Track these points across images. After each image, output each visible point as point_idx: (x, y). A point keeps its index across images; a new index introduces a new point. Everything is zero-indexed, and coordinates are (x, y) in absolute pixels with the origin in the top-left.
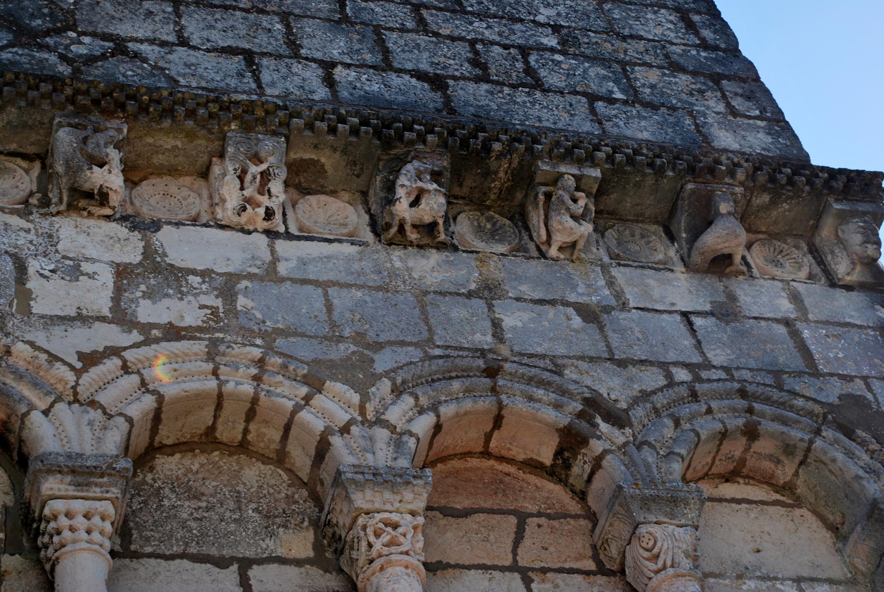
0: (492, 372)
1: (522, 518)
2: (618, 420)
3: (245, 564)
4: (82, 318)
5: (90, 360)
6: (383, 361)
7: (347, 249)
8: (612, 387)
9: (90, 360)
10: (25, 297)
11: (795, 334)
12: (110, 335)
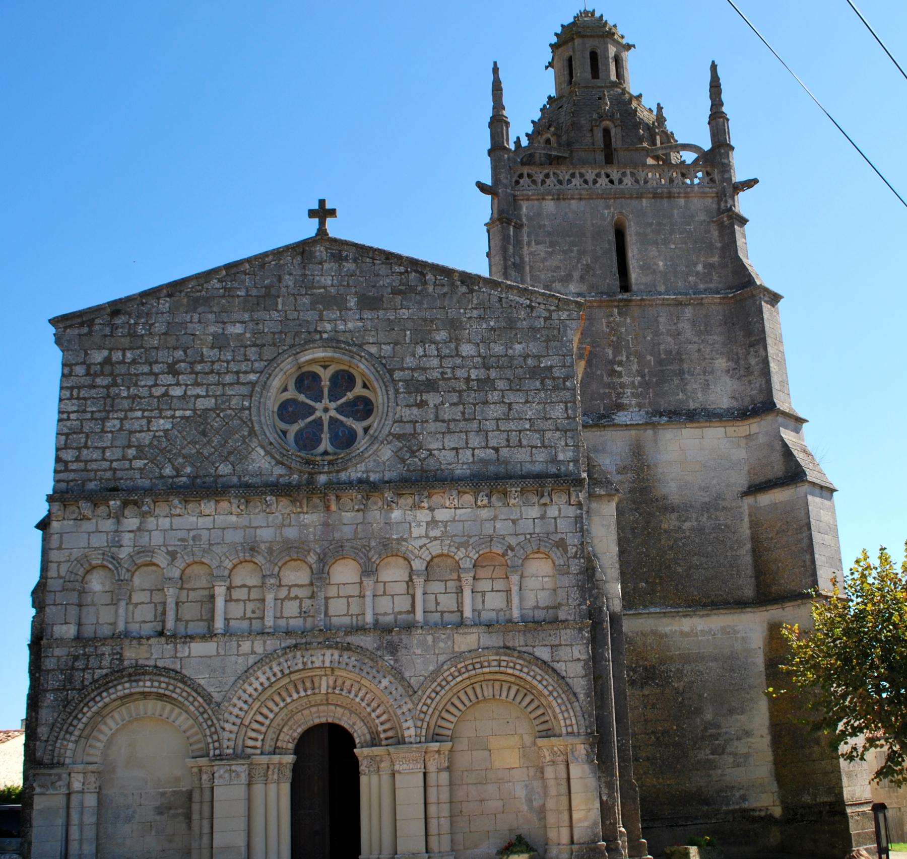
0: (491, 541)
1: (495, 566)
2: (512, 550)
3: (446, 581)
4: (420, 537)
5: (421, 547)
6: (471, 541)
7: (470, 510)
8: (513, 541)
9: (421, 547)
10: (411, 532)
11: (556, 522)
12: (425, 541)
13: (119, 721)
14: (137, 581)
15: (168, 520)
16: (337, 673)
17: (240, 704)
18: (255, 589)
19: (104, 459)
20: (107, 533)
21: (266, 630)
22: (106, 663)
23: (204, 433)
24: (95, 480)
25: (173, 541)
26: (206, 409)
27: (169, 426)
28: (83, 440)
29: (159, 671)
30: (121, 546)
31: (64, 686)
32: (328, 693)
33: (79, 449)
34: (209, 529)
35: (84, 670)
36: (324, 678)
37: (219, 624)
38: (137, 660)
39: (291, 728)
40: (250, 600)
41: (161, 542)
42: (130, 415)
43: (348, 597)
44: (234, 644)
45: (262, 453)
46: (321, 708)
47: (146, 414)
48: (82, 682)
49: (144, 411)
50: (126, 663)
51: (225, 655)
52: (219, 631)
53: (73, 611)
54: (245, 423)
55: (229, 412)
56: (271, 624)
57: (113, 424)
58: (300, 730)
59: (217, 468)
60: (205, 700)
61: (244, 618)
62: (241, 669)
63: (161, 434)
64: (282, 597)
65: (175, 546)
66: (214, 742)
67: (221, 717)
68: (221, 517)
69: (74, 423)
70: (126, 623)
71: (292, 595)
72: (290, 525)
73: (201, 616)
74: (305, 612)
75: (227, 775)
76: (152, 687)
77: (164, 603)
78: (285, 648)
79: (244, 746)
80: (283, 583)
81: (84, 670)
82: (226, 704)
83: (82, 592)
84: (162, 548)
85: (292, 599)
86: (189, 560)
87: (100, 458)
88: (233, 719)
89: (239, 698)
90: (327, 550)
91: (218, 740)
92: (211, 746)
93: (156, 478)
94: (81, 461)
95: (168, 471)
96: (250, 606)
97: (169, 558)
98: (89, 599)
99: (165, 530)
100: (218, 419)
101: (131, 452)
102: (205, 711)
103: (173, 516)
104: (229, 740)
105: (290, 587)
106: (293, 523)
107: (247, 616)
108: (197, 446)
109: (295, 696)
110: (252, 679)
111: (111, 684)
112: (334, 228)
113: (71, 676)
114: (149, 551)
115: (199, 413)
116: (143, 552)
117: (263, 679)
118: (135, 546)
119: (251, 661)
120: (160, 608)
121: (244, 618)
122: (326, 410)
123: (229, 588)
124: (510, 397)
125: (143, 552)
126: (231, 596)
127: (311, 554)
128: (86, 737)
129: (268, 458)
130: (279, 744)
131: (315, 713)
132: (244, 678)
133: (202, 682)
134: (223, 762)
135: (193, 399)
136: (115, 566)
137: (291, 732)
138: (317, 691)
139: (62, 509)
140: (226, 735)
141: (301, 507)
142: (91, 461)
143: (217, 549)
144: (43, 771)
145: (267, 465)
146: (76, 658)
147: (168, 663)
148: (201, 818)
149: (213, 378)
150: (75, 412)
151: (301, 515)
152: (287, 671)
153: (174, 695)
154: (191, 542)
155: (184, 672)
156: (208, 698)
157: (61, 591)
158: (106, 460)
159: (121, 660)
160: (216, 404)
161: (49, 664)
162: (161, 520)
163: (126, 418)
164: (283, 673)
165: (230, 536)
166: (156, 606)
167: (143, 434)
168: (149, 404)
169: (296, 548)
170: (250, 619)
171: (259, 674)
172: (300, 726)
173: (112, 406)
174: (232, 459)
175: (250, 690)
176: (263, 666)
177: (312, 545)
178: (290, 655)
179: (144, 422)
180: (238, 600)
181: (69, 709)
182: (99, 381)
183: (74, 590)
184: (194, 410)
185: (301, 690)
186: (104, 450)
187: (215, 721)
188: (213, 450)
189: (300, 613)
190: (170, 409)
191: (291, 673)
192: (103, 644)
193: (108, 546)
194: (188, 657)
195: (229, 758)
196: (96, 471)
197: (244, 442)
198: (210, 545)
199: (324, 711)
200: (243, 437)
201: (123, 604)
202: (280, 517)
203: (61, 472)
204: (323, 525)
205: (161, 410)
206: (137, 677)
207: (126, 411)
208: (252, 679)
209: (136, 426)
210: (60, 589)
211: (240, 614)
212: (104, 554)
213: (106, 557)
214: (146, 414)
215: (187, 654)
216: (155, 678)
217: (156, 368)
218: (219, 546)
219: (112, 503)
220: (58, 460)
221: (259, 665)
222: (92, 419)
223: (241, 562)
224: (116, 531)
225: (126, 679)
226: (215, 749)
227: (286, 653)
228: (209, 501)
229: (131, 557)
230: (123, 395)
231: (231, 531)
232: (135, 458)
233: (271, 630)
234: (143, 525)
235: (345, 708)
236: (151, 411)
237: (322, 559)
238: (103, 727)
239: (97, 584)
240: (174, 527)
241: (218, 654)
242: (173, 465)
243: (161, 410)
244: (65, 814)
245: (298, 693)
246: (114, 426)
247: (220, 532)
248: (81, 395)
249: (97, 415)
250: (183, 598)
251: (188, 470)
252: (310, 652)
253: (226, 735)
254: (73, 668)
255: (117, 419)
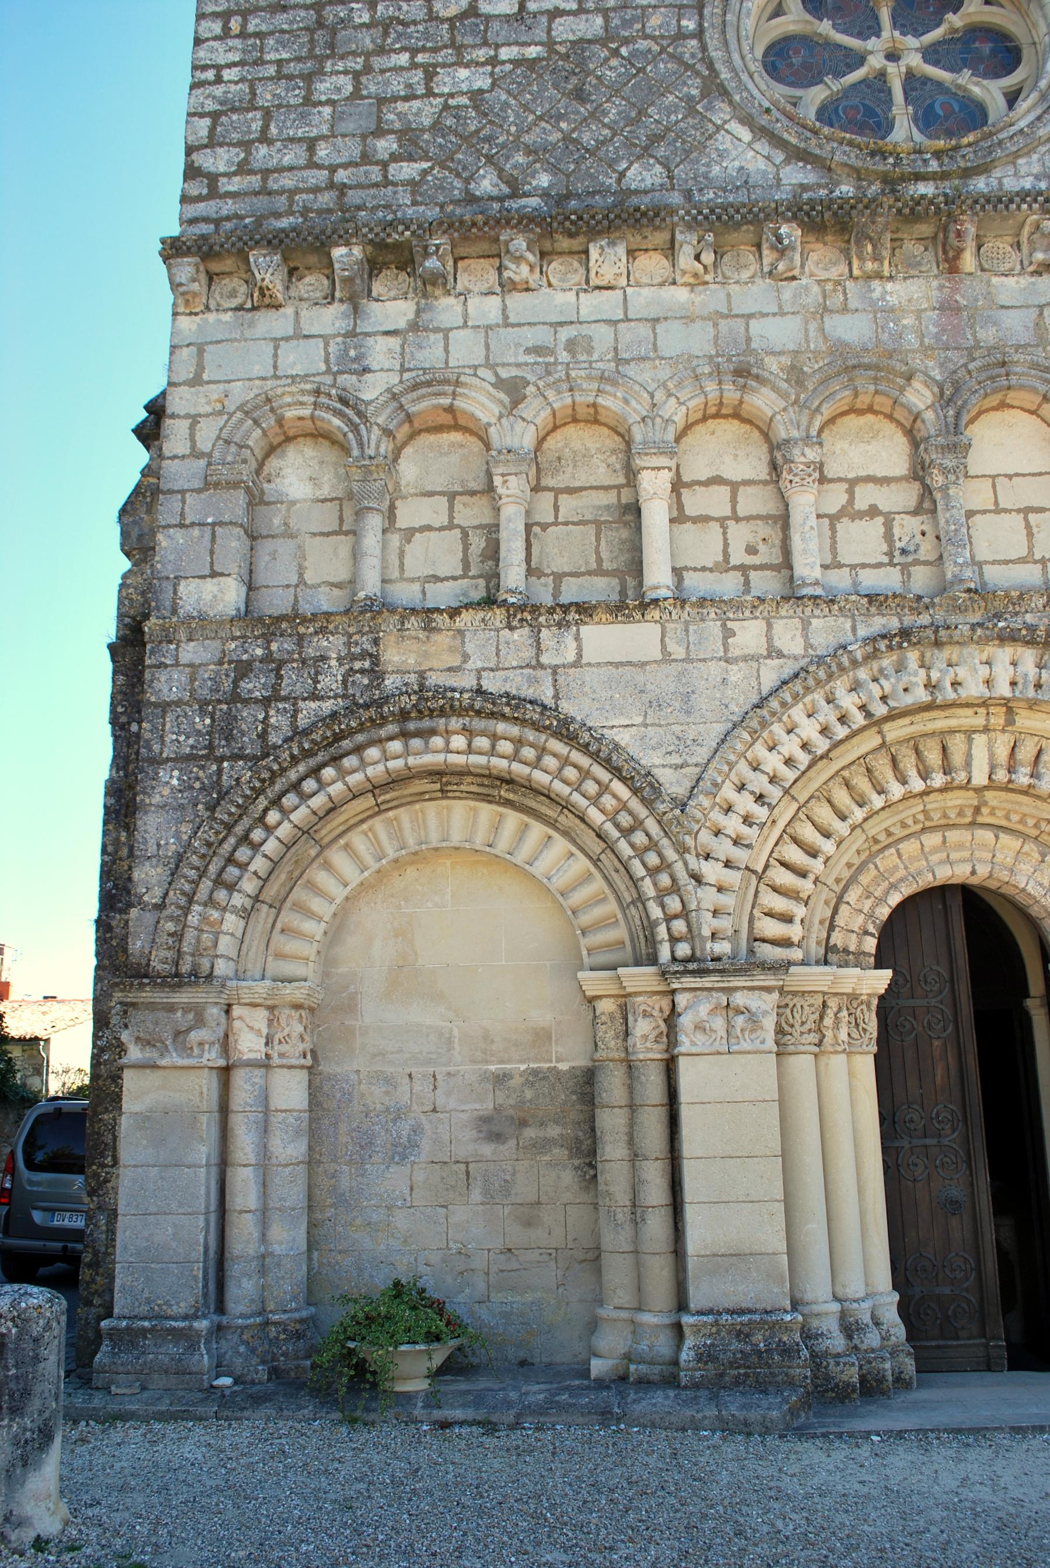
13: (369, 860)
14: (409, 469)
15: (495, 301)
16: (1025, 720)
17: (745, 803)
18: (750, 490)
19: (312, 165)
20: (326, 339)
21: (806, 591)
22: (330, 681)
23: (580, 95)
24: (291, 213)
25: (511, 353)
26: (581, 40)
27: (485, 83)
28: (257, 126)
29: (486, 706)
30: (366, 370)
31: (211, 747)
32: (992, 785)
33: (246, 145)
34: (614, 323)
35: (266, 702)
36: (980, 740)
37: (658, 576)
38: (422, 675)
39: (869, 895)
40: (737, 519)
41: (478, 356)
42: (377, 62)
43: (1026, 511)
44: (714, 628)
45: (746, 135)
46: (953, 836)
47: (420, 58)
48: (263, 736)
49: (414, 52)
50: (390, 682)
51: (687, 660)
52: (663, 593)
53: (233, 542)
54: (688, 67)
55: (642, 45)
56: (817, 573)
57: (334, 84)
58: (895, 899)
59: (622, 175)
60: (635, 791)
61: (725, 566)
62: (740, 701)
63: (464, 100)
64: (833, 510)
65: (518, 365)
66: (669, 919)
67: (689, 841)
68: (645, 291)
69: (233, 88)
70: (383, 581)
71: (861, 504)
72: (845, 309)
73: (599, 560)
74: (904, 552)
75: (719, 1023)
76: (470, 750)
77: (492, 530)
78: (874, 640)
79: (755, 939)
80: (830, 472)
81: (266, 702)
82: (706, 802)
83: (256, 500)
84: (481, 372)
85: (860, 515)
86: (561, 401)
87: (302, 162)
88: (724, 848)
89: (741, 788)
90: (962, 373)
91: (685, 914)
92: (662, 931)
93: (456, 202)
94: (252, 172)
95: (487, 184)
96: (740, 535)
97: (502, 396)
98: (276, 521)
99: (488, 328)
100: (614, 62)
101: (385, 146)
102: (638, 825)
103: (508, 287)
104: (715, 913)
105: (853, 483)
106: (853, 304)
107: (734, 561)
108: (563, 125)
109: (896, 791)
110: (778, 729)
111: (346, 744)
113: (231, 719)
114: (446, 382)
115: (562, 50)
116: (429, 384)
117: (809, 730)
118: (403, 370)
119: (769, 678)
120: (477, 543)
121: (725, 566)
123: (678, 486)
125: (429, 384)
126: (680, 506)
127: (916, 384)
128: (270, 903)
129: (763, 147)
130: (837, 939)
131: (935, 850)
132: (755, 724)
133: (623, 738)
134: (707, 982)
135: (544, 19)
136: (349, 422)
137: (867, 905)
138: (961, 777)
139: (203, 277)
140: (708, 897)
141: (877, 258)
142: (280, 170)
143: (642, 374)
144: (148, 995)
145: (762, 164)
146: (244, 669)
147: (516, 684)
148: (635, 1157)
150: (234, 64)
151: (876, 284)
152: (880, 710)
153: (540, 777)
154: (564, 356)
155: (567, 707)
156: (644, 786)
157: (199, 491)
158: (319, 167)
159: (376, 674)
160: (606, 28)
161: (166, 685)
162: (473, 302)
163: (368, 69)
164: (869, 715)
165: (674, 340)
166: (465, 535)
167: (416, 104)
168: (427, 35)
169: (868, 367)
170: (743, 569)
171: (797, 712)
172: (893, 886)
173: (332, 46)
174: (661, 151)
175: (773, 762)
176: (808, 690)
177: (917, 362)
178: (887, 662)
179: (418, 76)
180: (704, 519)
181: (227, 815)
183: (235, 485)
184: (550, 44)
185: (912, 773)
186: (311, 144)
187: (671, 855)
188: (606, 132)
189: (890, 554)
190: (485, 43)
191: (892, 716)
192: (322, 631)
193: (329, 371)
194: (577, 664)
195: (718, 966)
196: (293, 192)
197: (691, 111)
198: (619, 361)
199: (960, 846)
200: (689, 99)
201: (374, 522)
202: (816, 289)
203: (199, 199)
204: (942, 308)
205: (459, 49)
206: (426, 723)
207: (368, 55)
208: (778, 729)
209: (397, 86)
210: (197, 484)
211: (712, 555)
212: (317, 392)
213: (323, 399)
214: (420, 58)
215: (571, 657)
216: (478, 724)
218: (648, 364)
219: (338, 252)
220: (192, 172)
221: (798, 686)
222: (279, 76)
223: (705, 419)
224: (352, 334)
225: (392, 728)
226: (674, 940)
227: (874, 655)
228: (612, 244)
229: (394, 397)
230: (357, 21)
231: (675, 326)
232: (395, 158)
233: (819, 591)
234: (425, 316)
235: (1025, 837)
236: (435, 50)
237: (951, 397)
238: (322, 878)
239: (300, 478)
240: (511, 320)
241: (667, 657)
242: (500, 171)
243: (459, 49)
244: (214, 1132)
245: (904, 782)
246: (338, 90)
247: (644, 330)
248: (251, 28)
249: (293, 68)
250: (544, 509)
251: (544, 180)
252: (946, 653)
253: (708, 897)
254: (235, 697)
255: (345, 72)
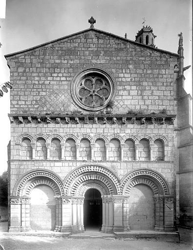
112: (96, 26)
122: (94, 92)
124: (153, 88)
149: (58, 79)
182: (22, 78)
203: (12, 108)
217: (40, 74)
